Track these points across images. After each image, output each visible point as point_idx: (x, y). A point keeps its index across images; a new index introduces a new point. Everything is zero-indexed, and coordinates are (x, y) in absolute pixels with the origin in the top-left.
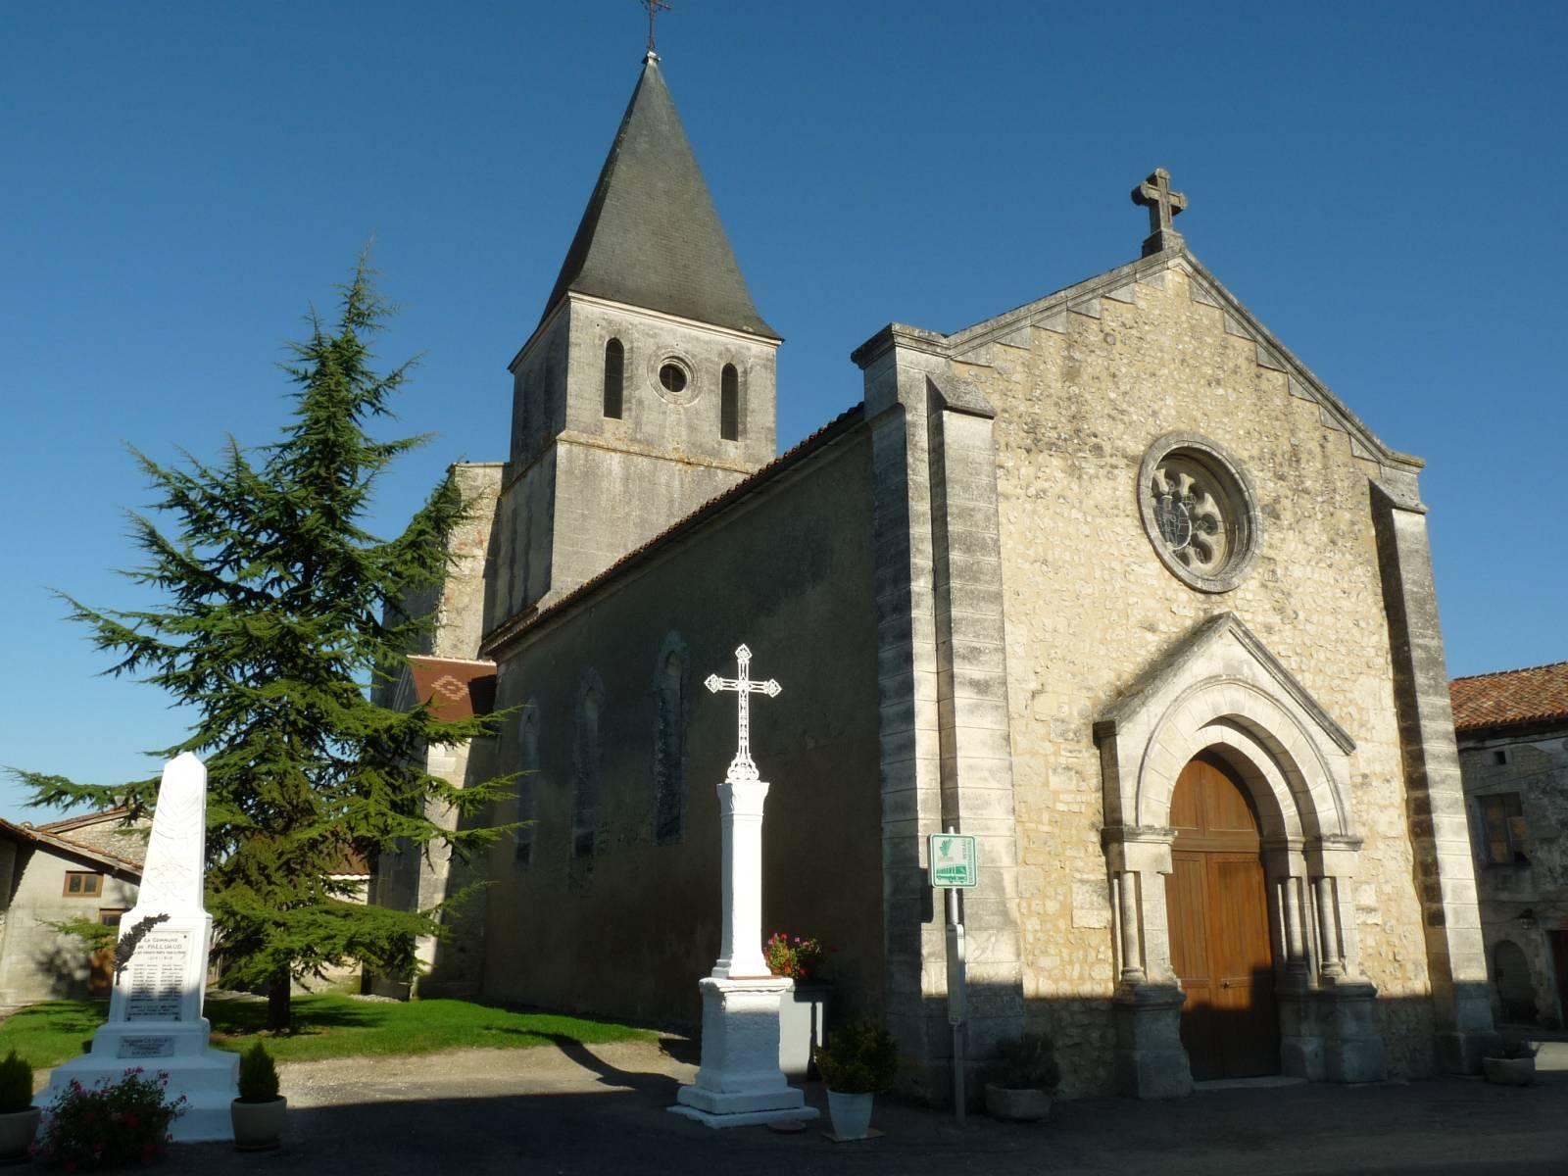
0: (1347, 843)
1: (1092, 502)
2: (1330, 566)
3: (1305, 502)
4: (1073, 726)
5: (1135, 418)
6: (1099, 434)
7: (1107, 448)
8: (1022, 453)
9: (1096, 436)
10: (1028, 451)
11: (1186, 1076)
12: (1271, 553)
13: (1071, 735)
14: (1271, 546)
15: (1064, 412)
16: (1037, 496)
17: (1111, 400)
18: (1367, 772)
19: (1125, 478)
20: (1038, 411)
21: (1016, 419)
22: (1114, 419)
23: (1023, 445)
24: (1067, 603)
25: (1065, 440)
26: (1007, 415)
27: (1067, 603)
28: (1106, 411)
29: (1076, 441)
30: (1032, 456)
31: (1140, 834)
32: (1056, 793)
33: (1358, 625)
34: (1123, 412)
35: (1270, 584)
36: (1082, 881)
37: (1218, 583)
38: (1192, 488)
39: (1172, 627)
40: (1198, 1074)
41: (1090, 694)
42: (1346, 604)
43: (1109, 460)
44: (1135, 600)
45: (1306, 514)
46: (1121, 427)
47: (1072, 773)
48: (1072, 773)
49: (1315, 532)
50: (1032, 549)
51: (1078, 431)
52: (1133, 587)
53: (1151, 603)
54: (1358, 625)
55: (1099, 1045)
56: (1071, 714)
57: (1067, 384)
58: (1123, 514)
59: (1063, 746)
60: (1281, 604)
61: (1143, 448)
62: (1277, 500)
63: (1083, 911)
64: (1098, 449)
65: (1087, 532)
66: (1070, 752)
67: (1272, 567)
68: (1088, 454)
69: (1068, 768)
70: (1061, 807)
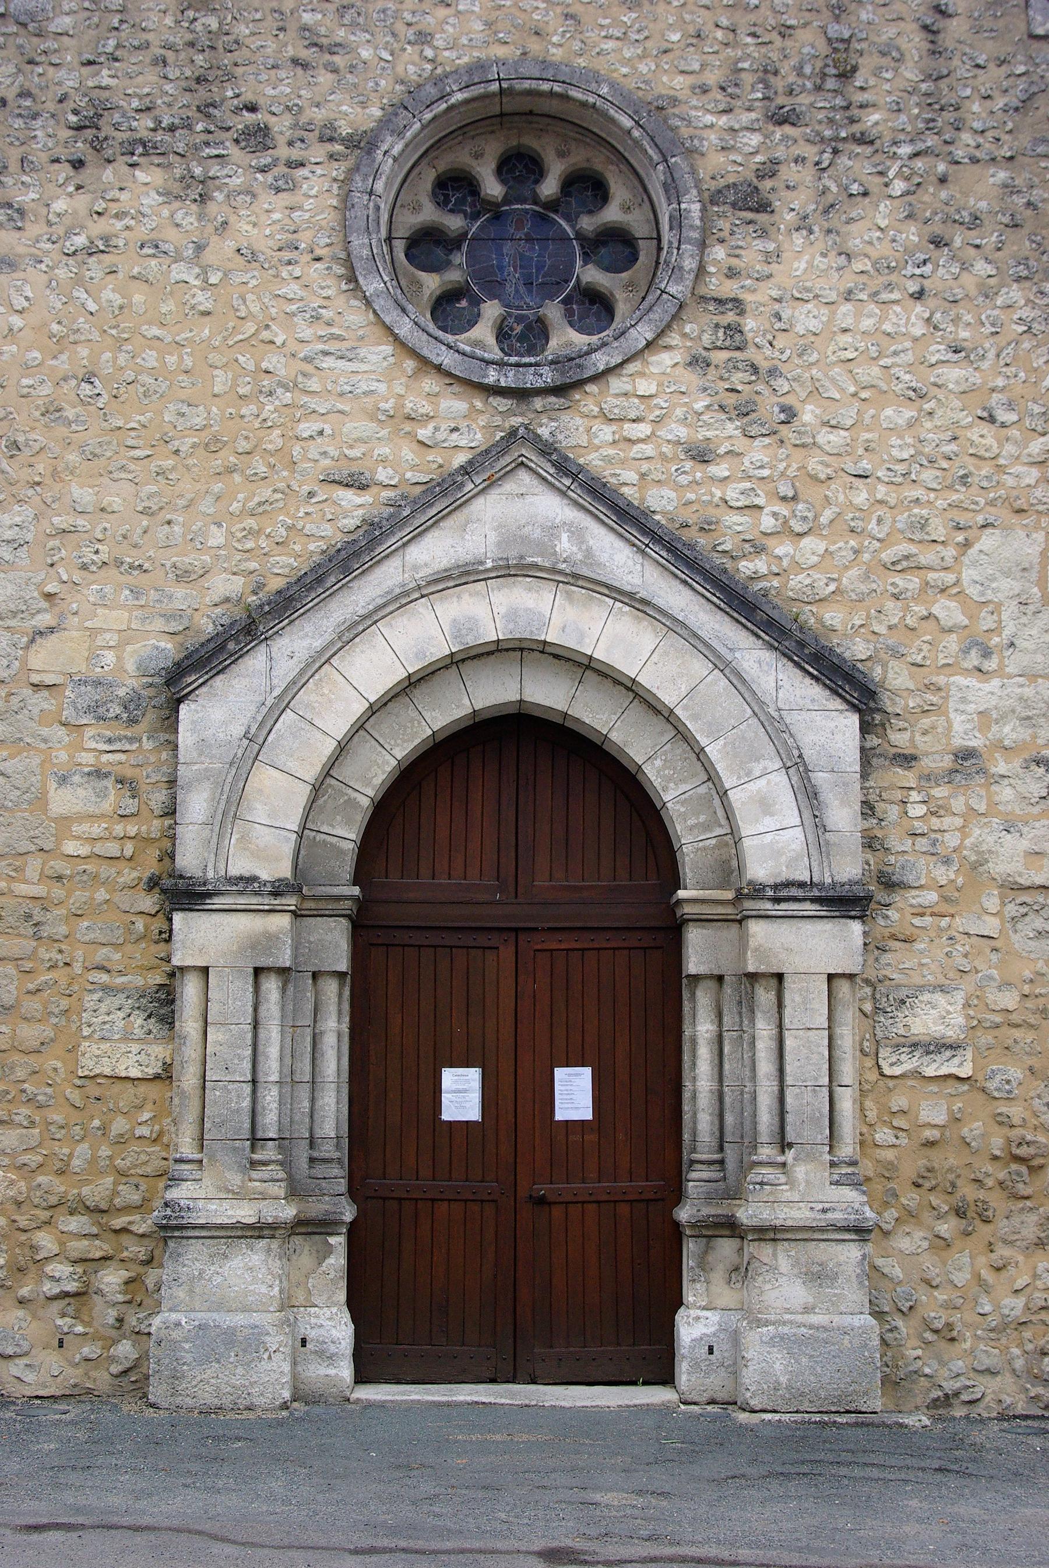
0: (814, 900)
1: (231, 245)
2: (919, 296)
3: (857, 165)
4: (121, 692)
5: (365, 53)
6: (262, 102)
7: (281, 126)
8: (64, 171)
9: (252, 108)
10: (78, 164)
11: (345, 1371)
12: (728, 288)
13: (116, 709)
14: (732, 273)
15: (173, 73)
16: (91, 251)
17: (305, 28)
18: (975, 742)
19: (317, 189)
20: (106, 81)
21: (51, 106)
22: (305, 66)
23: (63, 153)
24: (138, 453)
25: (172, 129)
26: (28, 103)
27: (138, 453)
28: (290, 51)
29: (199, 127)
30: (86, 175)
31: (209, 895)
32: (65, 821)
33: (992, 419)
34: (332, 49)
35: (720, 357)
36: (107, 990)
37: (545, 370)
38: (505, 168)
39: (400, 465)
40: (361, 1378)
41: (175, 626)
42: (954, 375)
43: (283, 152)
44: (316, 426)
45: (855, 188)
46: (325, 78)
47: (109, 783)
48: (109, 783)
49: (880, 227)
50: (64, 357)
51: (205, 109)
52: (313, 403)
53: (359, 427)
54: (992, 419)
55: (120, 1298)
56: (120, 667)
57: (191, 14)
58: (308, 257)
59: (89, 732)
60: (743, 398)
61: (378, 113)
62: (770, 170)
63: (105, 1046)
64: (258, 138)
65: (207, 306)
66: (110, 741)
67: (730, 317)
68: (233, 151)
69: (98, 774)
70: (71, 847)
